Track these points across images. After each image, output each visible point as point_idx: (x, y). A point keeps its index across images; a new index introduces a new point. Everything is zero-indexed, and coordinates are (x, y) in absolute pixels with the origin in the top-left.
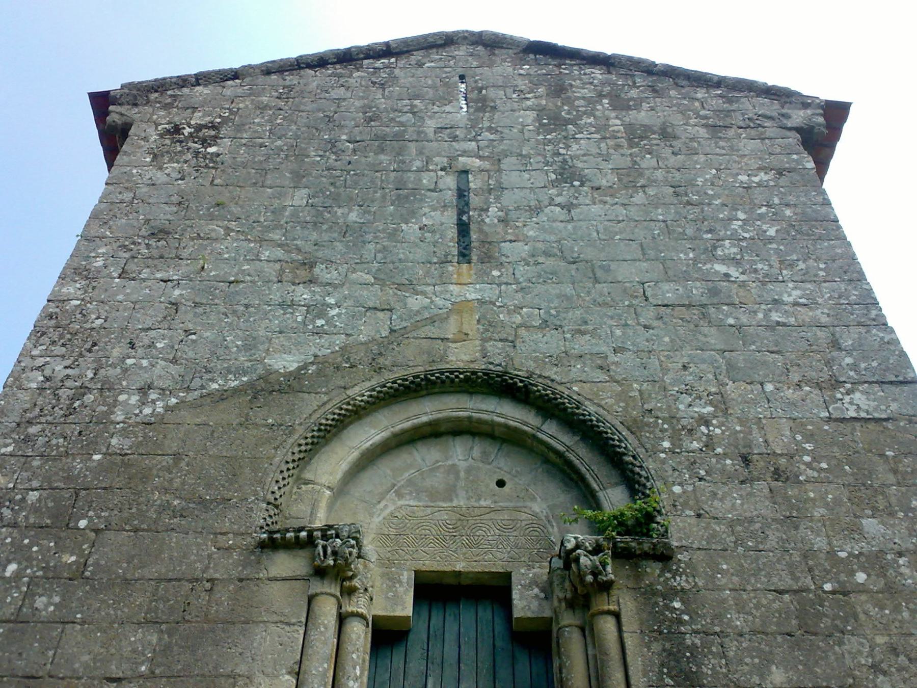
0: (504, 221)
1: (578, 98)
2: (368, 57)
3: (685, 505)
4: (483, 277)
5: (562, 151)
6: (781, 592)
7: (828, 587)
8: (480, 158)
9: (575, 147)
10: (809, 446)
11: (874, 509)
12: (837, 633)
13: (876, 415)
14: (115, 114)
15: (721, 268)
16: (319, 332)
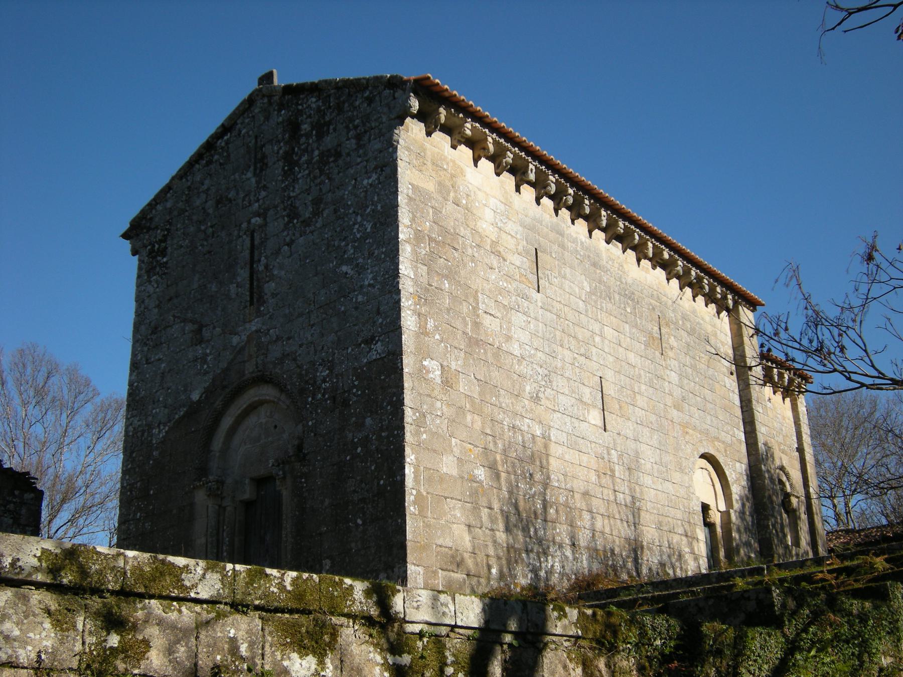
1: (302, 135)
2: (218, 139)
3: (312, 431)
4: (259, 314)
5: (292, 194)
7: (348, 458)
8: (259, 216)
9: (297, 186)
10: (356, 383)
13: (383, 355)
15: (344, 268)
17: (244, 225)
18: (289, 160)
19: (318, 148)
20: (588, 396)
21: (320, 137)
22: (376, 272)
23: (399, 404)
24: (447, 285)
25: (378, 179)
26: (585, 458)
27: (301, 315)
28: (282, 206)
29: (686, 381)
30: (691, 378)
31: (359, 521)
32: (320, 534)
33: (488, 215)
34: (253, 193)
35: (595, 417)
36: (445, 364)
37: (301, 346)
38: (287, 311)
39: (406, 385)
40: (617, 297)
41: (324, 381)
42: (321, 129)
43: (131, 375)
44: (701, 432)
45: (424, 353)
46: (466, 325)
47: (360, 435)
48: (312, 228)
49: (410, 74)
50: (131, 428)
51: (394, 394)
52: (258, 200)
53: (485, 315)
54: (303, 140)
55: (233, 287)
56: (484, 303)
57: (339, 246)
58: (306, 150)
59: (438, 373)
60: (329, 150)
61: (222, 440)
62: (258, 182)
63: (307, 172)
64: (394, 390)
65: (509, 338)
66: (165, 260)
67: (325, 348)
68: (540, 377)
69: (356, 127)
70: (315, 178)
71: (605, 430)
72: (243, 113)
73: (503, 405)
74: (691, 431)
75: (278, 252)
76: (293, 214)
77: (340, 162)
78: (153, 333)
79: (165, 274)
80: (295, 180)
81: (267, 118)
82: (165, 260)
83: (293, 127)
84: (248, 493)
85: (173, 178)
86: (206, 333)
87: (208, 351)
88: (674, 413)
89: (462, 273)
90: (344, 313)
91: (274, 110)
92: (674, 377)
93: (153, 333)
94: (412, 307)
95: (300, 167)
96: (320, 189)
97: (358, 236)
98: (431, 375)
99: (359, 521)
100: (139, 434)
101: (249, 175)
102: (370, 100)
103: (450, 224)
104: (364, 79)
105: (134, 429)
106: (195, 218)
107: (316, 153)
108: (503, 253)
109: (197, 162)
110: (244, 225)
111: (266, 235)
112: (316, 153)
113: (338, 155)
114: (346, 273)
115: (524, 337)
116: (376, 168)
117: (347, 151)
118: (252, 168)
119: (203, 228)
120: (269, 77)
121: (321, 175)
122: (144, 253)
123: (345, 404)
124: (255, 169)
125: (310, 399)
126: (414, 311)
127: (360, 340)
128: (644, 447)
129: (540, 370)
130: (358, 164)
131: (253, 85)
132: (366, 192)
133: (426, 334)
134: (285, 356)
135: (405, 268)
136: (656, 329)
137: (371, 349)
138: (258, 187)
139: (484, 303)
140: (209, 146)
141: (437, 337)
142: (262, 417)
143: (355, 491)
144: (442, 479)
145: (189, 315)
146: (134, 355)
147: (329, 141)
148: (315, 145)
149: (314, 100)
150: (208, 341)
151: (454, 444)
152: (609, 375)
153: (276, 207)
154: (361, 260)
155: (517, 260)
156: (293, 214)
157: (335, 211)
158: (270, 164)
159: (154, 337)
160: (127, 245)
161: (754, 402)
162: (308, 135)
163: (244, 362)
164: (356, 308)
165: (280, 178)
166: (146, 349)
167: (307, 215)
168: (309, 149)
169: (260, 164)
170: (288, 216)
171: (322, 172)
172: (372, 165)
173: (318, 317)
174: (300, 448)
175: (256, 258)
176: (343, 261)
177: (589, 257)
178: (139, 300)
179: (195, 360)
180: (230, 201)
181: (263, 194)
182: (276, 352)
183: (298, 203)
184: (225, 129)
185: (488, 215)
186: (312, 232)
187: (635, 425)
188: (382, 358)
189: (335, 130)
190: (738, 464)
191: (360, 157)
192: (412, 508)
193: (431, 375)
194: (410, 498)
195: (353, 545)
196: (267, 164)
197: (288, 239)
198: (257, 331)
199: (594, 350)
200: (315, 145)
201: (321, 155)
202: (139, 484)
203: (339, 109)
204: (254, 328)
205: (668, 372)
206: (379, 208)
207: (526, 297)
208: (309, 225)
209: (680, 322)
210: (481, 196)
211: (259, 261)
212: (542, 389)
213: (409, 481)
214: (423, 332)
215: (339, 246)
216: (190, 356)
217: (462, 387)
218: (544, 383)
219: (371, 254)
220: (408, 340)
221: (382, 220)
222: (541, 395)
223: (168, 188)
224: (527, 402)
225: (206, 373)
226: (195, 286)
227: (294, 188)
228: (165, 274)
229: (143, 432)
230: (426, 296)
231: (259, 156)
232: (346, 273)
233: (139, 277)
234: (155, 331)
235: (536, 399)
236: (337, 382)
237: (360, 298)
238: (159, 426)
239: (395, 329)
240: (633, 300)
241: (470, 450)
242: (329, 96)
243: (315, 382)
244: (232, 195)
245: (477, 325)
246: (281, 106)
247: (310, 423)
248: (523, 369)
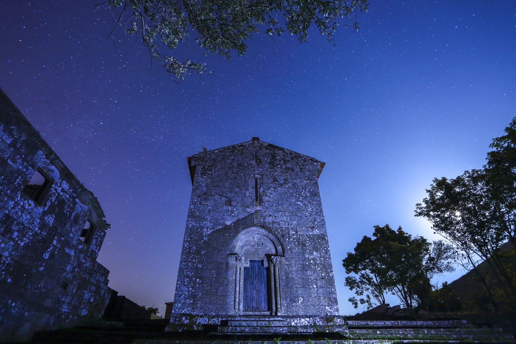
0: (264, 192)
4: (260, 205)
12: (307, 270)
14: (193, 163)
15: (299, 203)
16: (233, 217)
21: (285, 163)
31: (315, 286)
37: (282, 221)
42: (285, 162)
55: (248, 194)
69: (300, 166)
76: (275, 180)
99: (315, 286)
101: (253, 162)
123: (304, 245)
134: (273, 222)
145: (224, 195)
147: (289, 165)
156: (275, 180)
201: (286, 168)
202: (194, 248)
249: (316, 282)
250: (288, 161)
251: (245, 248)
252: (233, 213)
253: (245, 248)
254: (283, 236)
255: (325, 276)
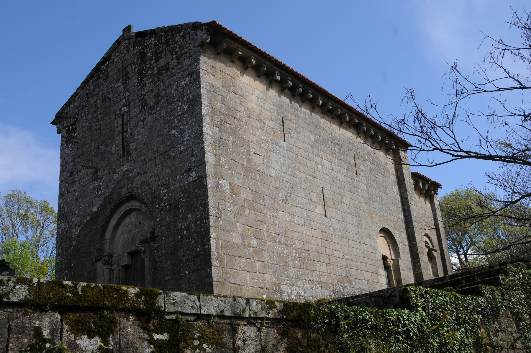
1: (147, 60)
3: (159, 224)
4: (128, 161)
5: (143, 93)
6: (171, 242)
9: (146, 88)
10: (182, 195)
11: (191, 211)
15: (173, 132)
17: (118, 112)
18: (141, 74)
19: (156, 66)
20: (316, 198)
21: (157, 60)
22: (191, 133)
23: (205, 206)
24: (231, 139)
25: (190, 81)
26: (315, 233)
27: (150, 160)
28: (138, 100)
29: (370, 189)
30: (373, 187)
31: (187, 272)
32: (166, 281)
33: (254, 99)
34: (122, 94)
35: (320, 210)
36: (232, 182)
37: (151, 177)
38: (143, 158)
39: (209, 194)
40: (330, 143)
41: (165, 195)
42: (157, 55)
43: (59, 200)
44: (380, 216)
45: (219, 176)
46: (243, 160)
47: (185, 224)
48: (155, 111)
49: (205, 20)
50: (60, 230)
51: (203, 200)
52: (125, 98)
53: (254, 155)
54: (148, 62)
55: (113, 147)
56: (253, 148)
57: (170, 120)
58: (150, 68)
59: (228, 187)
60: (162, 67)
61: (111, 233)
62: (124, 88)
63: (151, 80)
64: (203, 198)
65: (268, 167)
66: (76, 135)
67: (165, 177)
68: (288, 188)
69: (176, 53)
70: (155, 83)
71: (326, 217)
72: (115, 50)
73: (267, 204)
74: (374, 216)
75: (137, 125)
76: (144, 104)
77: (169, 73)
78: (71, 176)
79: (76, 142)
80: (145, 85)
81: (128, 52)
82: (76, 135)
83: (142, 55)
84: (126, 261)
85: (78, 89)
86: (100, 174)
87: (101, 184)
88: (364, 206)
89: (241, 131)
90: (174, 156)
91: (132, 47)
92: (364, 187)
93: (71, 176)
94: (211, 151)
95: (147, 78)
96: (158, 89)
97: (180, 113)
98: (224, 189)
99: (187, 272)
100: (65, 233)
101: (120, 84)
102: (183, 37)
103: (231, 105)
104: (180, 25)
105: (62, 230)
106: (91, 110)
107: (155, 69)
108: (263, 120)
109: (91, 79)
110: (118, 112)
111: (130, 116)
112: (155, 69)
113: (167, 69)
114: (174, 134)
115: (277, 166)
116: (188, 75)
117: (172, 66)
118: (121, 80)
119: (95, 115)
120: (128, 29)
121: (158, 81)
122: (64, 132)
123: (177, 207)
124: (123, 81)
125: (157, 206)
126: (213, 153)
127: (183, 171)
128: (348, 225)
129: (287, 185)
130: (178, 73)
131: (119, 33)
132: (183, 88)
133: (221, 166)
134: (143, 183)
135: (207, 129)
136: (353, 161)
137: (189, 176)
138: (124, 90)
139: (253, 148)
140: (97, 69)
141: (227, 167)
142: (132, 218)
143: (184, 256)
144: (232, 246)
146: (61, 189)
147: (162, 62)
148: (155, 65)
149: (153, 39)
150: (101, 178)
151: (238, 226)
152: (327, 187)
153: (135, 100)
154: (182, 127)
155: (272, 124)
157: (167, 100)
158: (130, 77)
159: (71, 178)
160: (54, 128)
161: (409, 199)
162: (151, 59)
163: (121, 188)
164: (181, 154)
165: (136, 84)
166: (67, 185)
167: (152, 104)
168: (152, 67)
169: (126, 78)
170: (142, 105)
171: (159, 79)
172: (186, 73)
173: (160, 160)
174: (153, 233)
175: (125, 130)
176: (172, 128)
177: (313, 122)
178: (63, 158)
179: (94, 189)
180: (110, 99)
181: (128, 94)
182: (138, 181)
183: (146, 98)
184: (106, 59)
185: (254, 99)
186: (155, 113)
187: (343, 213)
188: (196, 180)
189: (165, 55)
190: (402, 233)
191: (179, 69)
192: (215, 263)
193: (224, 189)
194: (214, 257)
195: (184, 286)
196: (129, 77)
197: (142, 118)
198: (127, 171)
199: (318, 173)
200: (155, 65)
203: (167, 44)
204: (125, 169)
205: (360, 184)
206: (191, 97)
207: (278, 145)
208: (153, 109)
209: (366, 157)
210: (249, 88)
211: (127, 131)
212: (289, 195)
213: (213, 248)
214: (218, 165)
215: (170, 120)
216: (92, 187)
217: (243, 194)
218: (290, 191)
219: (187, 123)
220: (209, 169)
221: (193, 103)
222: (288, 198)
223: (76, 94)
224: (280, 202)
225: (100, 196)
226: (93, 148)
227: (144, 89)
228: (76, 142)
229: (67, 231)
230: (219, 144)
231: (125, 73)
232: (174, 134)
233: (62, 145)
234: (71, 174)
235: (285, 201)
236: (172, 195)
237: (182, 148)
238: (75, 227)
239: (202, 163)
240: (339, 145)
241: (248, 230)
242: (161, 36)
243: (160, 196)
244: (111, 96)
245: (249, 160)
246: (135, 44)
247: (158, 220)
248: (278, 184)
249: (188, 264)
250: (162, 51)
251: (122, 238)
252: (100, 190)
253: (122, 238)
254: (153, 202)
255: (200, 251)
